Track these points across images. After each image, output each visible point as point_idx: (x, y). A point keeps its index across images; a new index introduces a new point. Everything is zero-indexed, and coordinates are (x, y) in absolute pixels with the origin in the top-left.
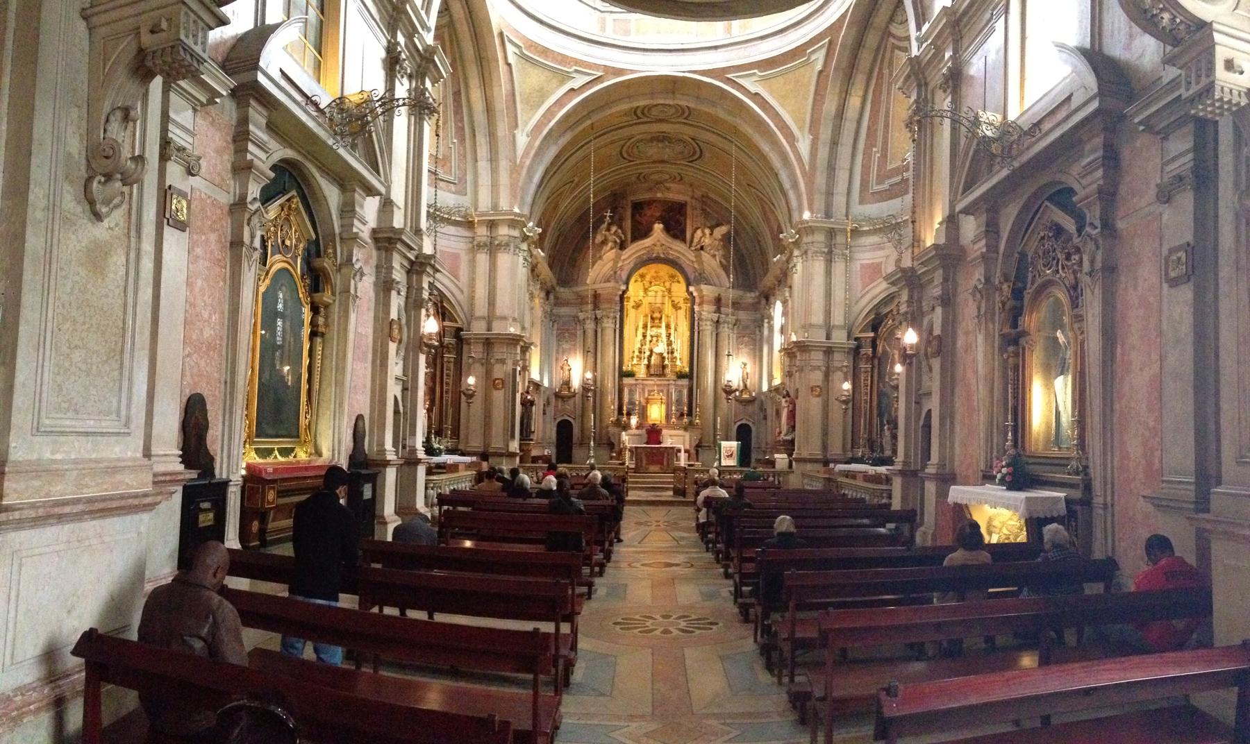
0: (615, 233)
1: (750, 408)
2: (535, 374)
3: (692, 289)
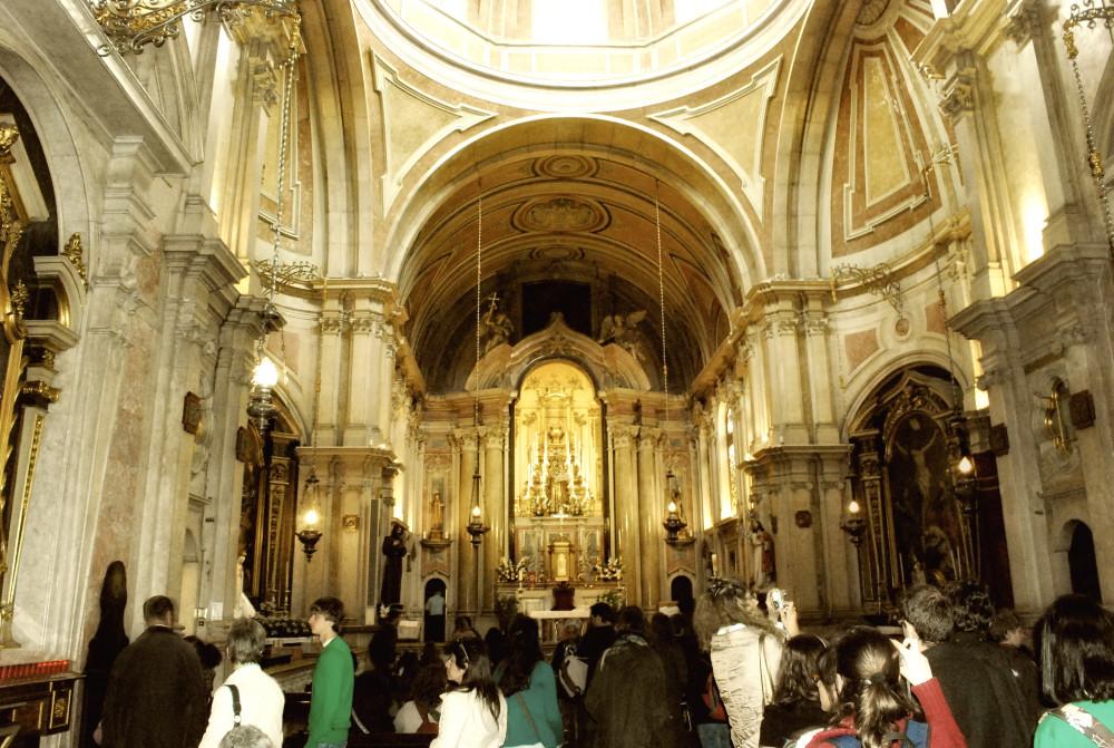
0: (502, 324)
1: (688, 553)
2: (397, 513)
3: (602, 394)
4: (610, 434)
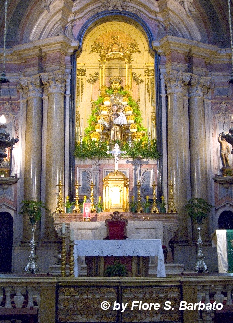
3: (156, 44)
4: (163, 81)
